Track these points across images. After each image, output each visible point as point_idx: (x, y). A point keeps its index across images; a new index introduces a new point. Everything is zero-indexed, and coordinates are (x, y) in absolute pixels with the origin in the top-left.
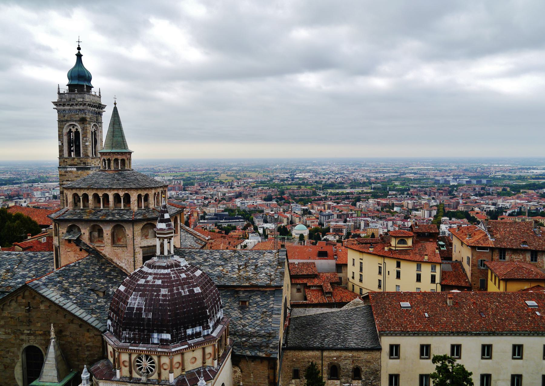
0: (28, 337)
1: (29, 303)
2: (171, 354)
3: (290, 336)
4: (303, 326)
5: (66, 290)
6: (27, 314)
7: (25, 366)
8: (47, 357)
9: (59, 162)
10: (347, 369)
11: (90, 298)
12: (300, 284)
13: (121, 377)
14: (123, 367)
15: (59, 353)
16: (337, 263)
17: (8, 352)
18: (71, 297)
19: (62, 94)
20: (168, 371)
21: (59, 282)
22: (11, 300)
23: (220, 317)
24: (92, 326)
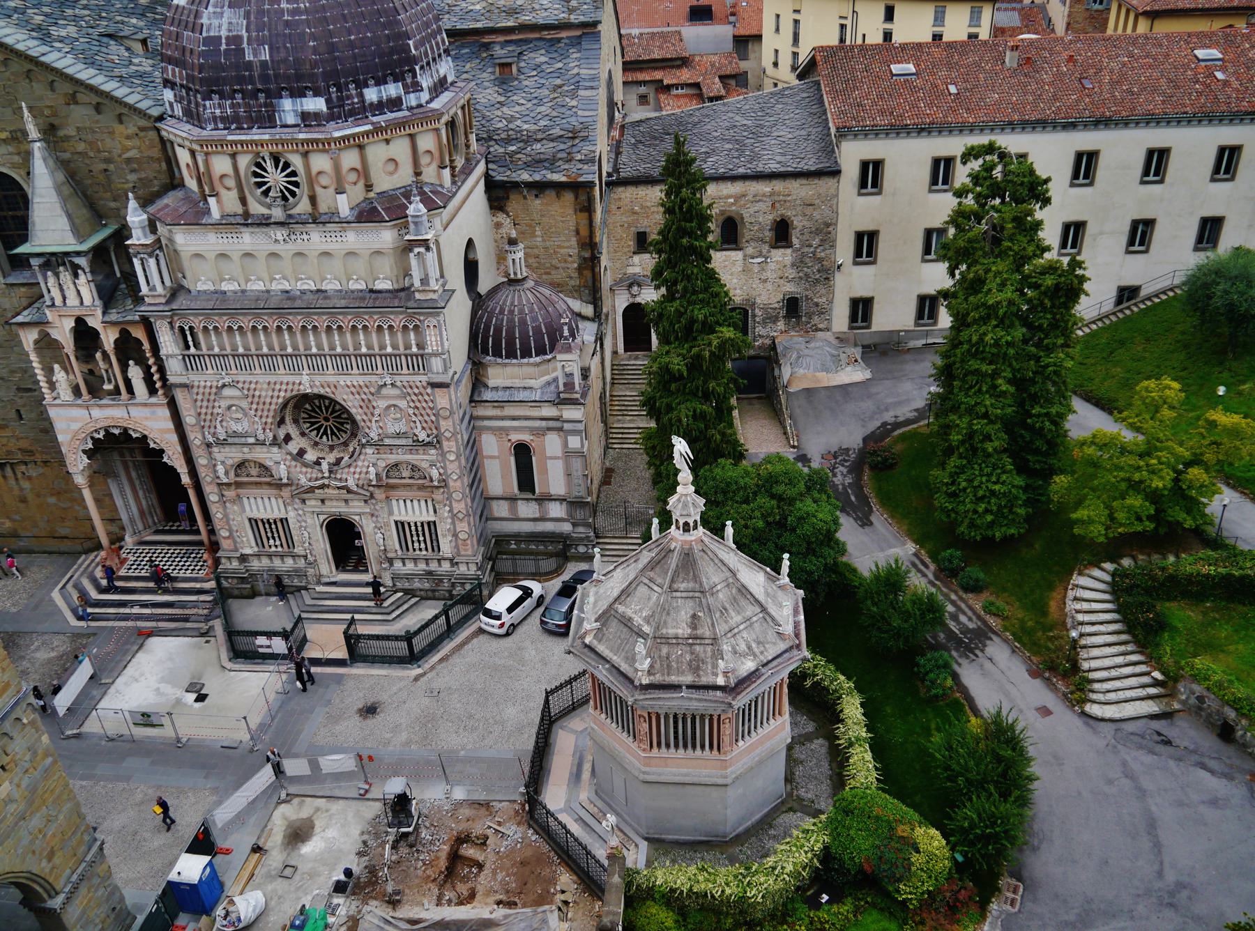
2: (333, 144)
3: (623, 158)
4: (655, 138)
5: (39, 28)
8: (33, 188)
10: (760, 224)
11: (110, 52)
12: (645, 83)
13: (222, 216)
14: (223, 192)
15: (61, 177)
16: (737, 34)
18: (57, 45)
20: (331, 190)
23: (445, 77)
24: (126, 105)
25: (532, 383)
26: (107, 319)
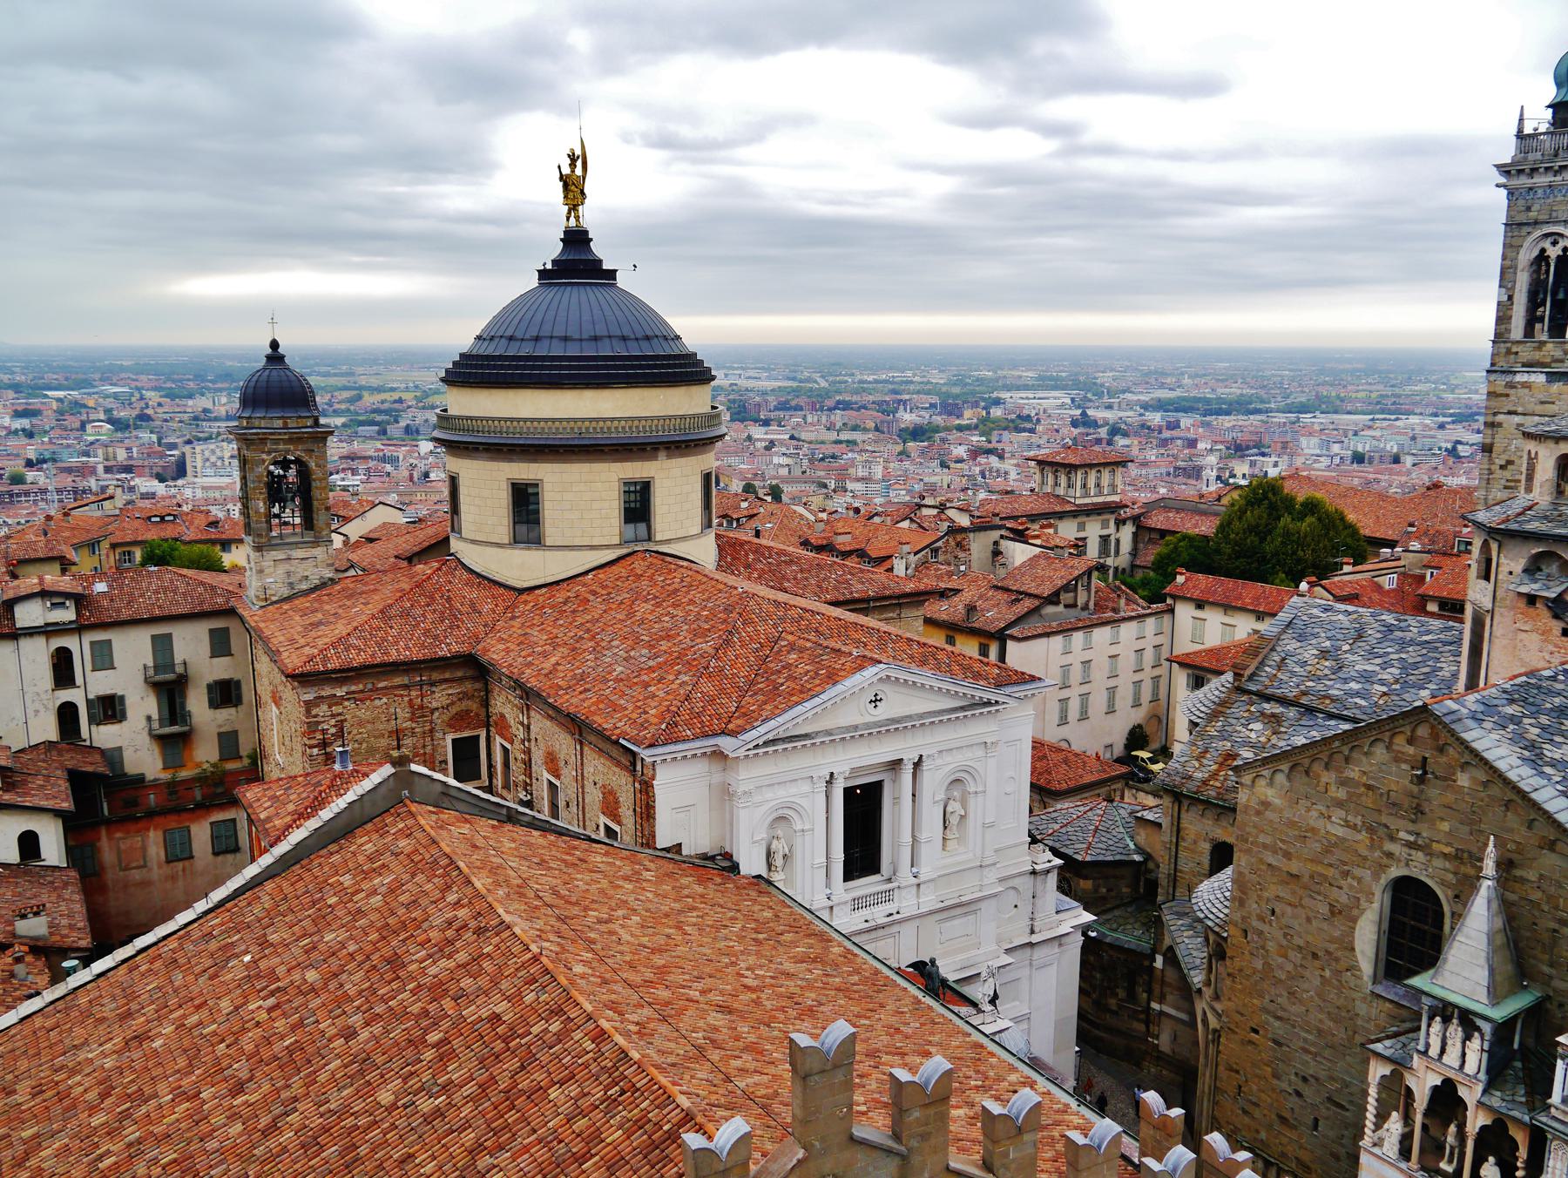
0: (1406, 850)
1: (1425, 759)
5: (1532, 746)
6: (1415, 789)
7: (1385, 926)
9: (1493, 355)
15: (1499, 923)
17: (1346, 874)
18: (1548, 770)
19: (1529, 135)
21: (1513, 719)
22: (1376, 740)
26: (1485, 1100)
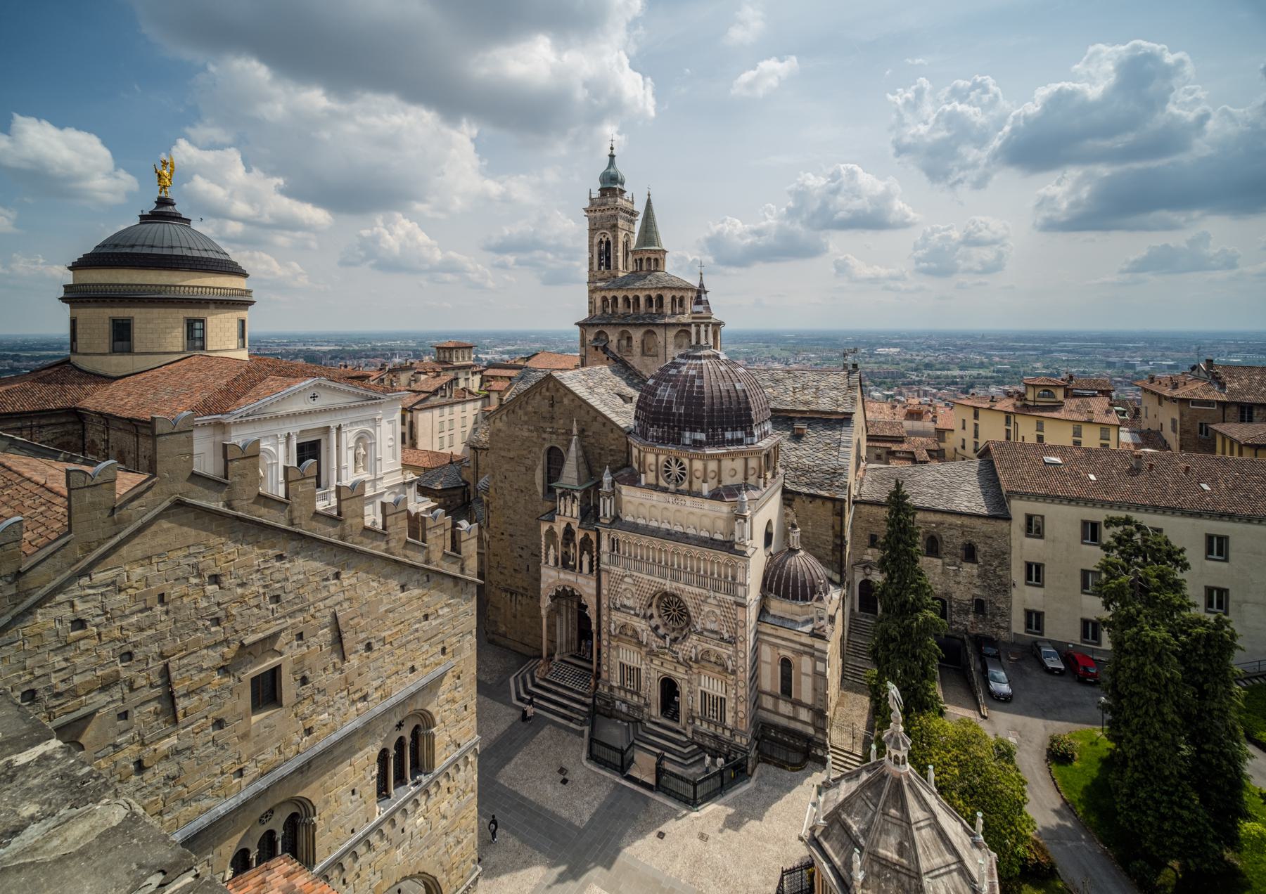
14: (649, 472)
15: (580, 453)
20: (701, 480)
25: (797, 618)
